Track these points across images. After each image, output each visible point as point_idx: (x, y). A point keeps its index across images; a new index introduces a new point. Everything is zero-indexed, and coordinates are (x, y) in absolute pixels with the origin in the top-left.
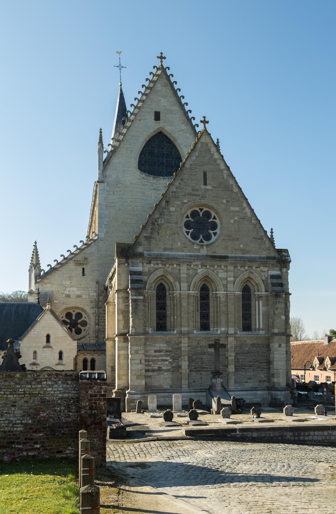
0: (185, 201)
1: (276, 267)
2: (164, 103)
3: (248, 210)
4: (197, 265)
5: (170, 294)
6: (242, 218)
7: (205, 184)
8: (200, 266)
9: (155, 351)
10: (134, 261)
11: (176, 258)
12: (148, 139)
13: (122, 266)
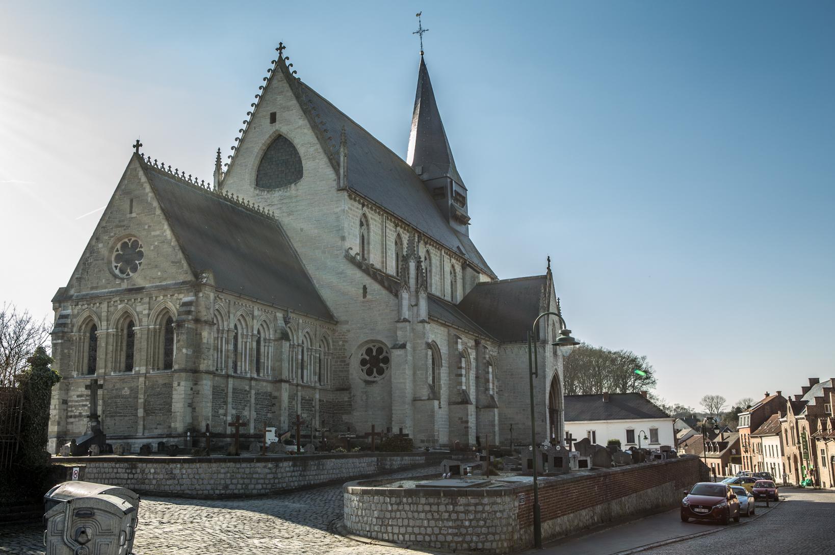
9: (78, 396)
11: (97, 297)
12: (264, 148)
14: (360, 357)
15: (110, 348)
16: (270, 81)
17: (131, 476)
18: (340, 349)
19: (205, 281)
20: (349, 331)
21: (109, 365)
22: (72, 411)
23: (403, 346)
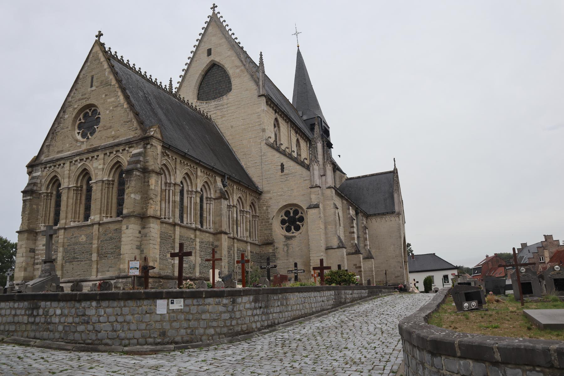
0: (76, 106)
6: (116, 107)
10: (37, 168)
12: (203, 73)
14: (280, 218)
15: (71, 201)
16: (206, 29)
17: (31, 320)
18: (265, 213)
19: (152, 134)
20: (271, 198)
21: (69, 216)
22: (38, 259)
23: (317, 206)
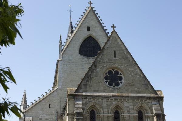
0: (105, 65)
1: (156, 100)
2: (92, 23)
3: (138, 70)
4: (113, 99)
5: (97, 115)
7: (115, 57)
8: (114, 100)
12: (84, 39)
13: (71, 100)
